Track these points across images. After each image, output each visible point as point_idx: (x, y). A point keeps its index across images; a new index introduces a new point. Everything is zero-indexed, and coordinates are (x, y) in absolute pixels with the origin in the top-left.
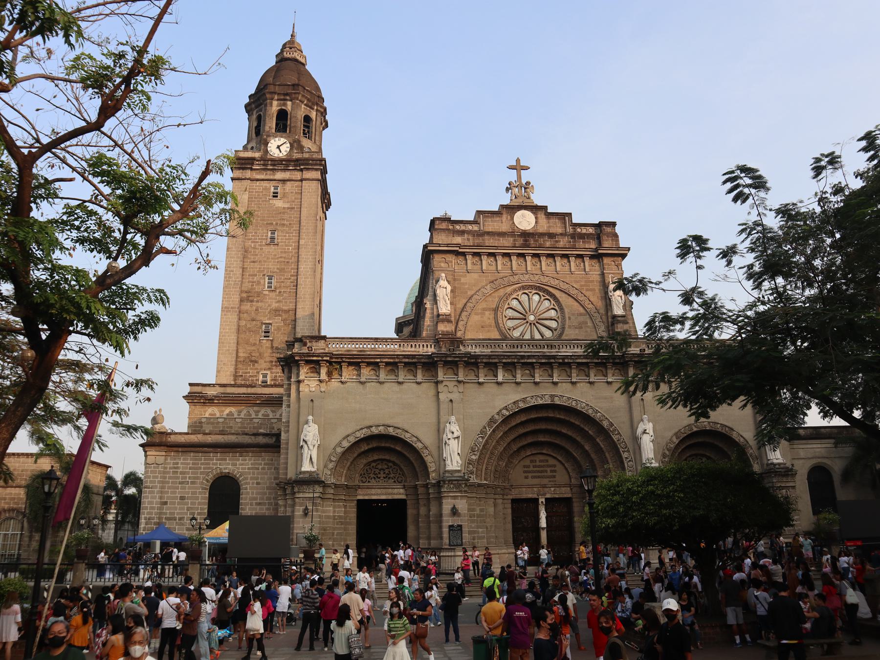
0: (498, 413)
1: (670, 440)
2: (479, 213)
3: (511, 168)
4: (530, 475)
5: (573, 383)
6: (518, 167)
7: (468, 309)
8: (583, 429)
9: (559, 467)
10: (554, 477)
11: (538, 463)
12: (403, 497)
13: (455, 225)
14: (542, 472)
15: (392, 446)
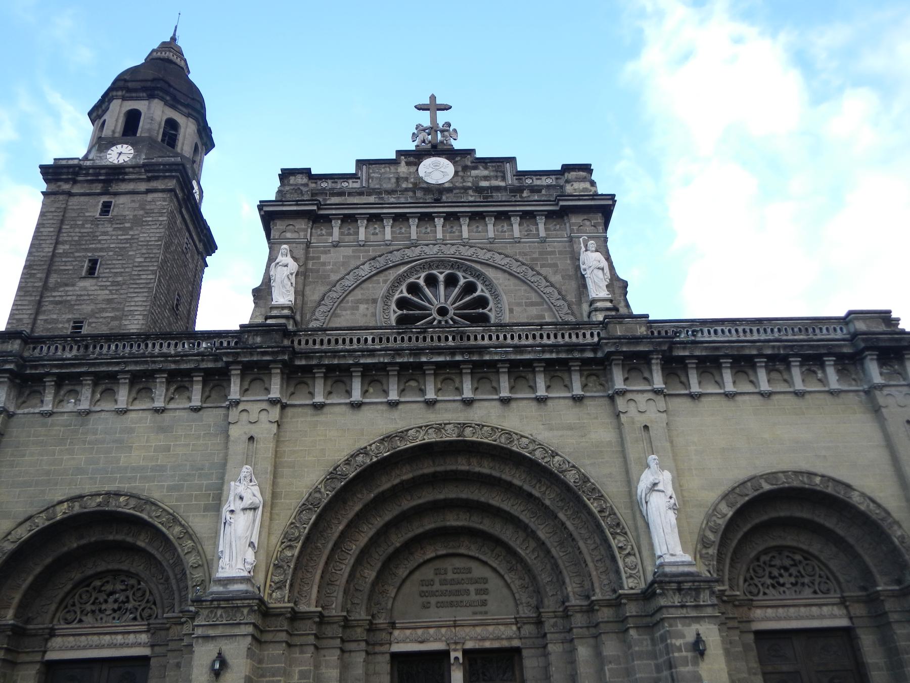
0: (347, 462)
1: (715, 510)
2: (360, 163)
3: (420, 108)
4: (433, 600)
5: (506, 401)
6: (433, 107)
7: (326, 301)
8: (530, 495)
9: (494, 582)
10: (484, 603)
11: (450, 576)
12: (146, 651)
13: (319, 182)
14: (458, 593)
15: (129, 539)
